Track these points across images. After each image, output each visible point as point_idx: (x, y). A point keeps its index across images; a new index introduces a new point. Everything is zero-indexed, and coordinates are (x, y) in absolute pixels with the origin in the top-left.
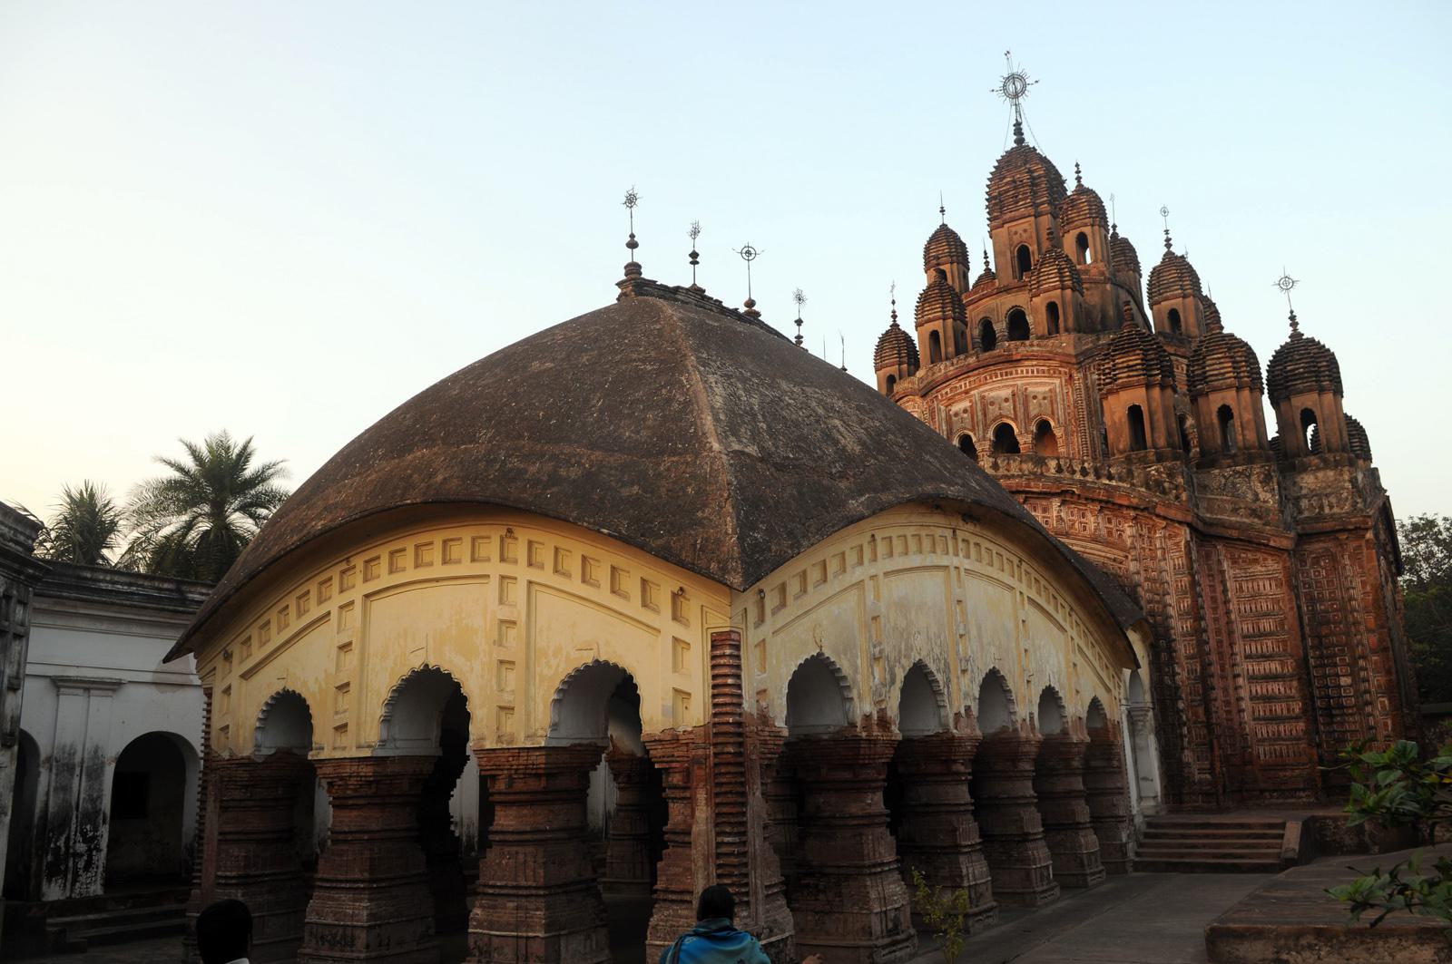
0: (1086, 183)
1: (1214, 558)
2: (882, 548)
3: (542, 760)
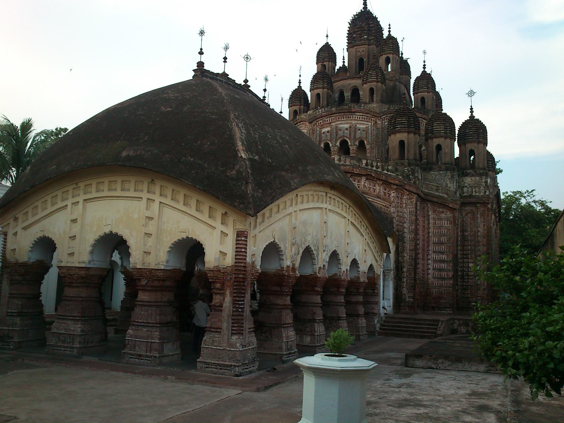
0: (393, 34)
1: (426, 209)
2: (299, 199)
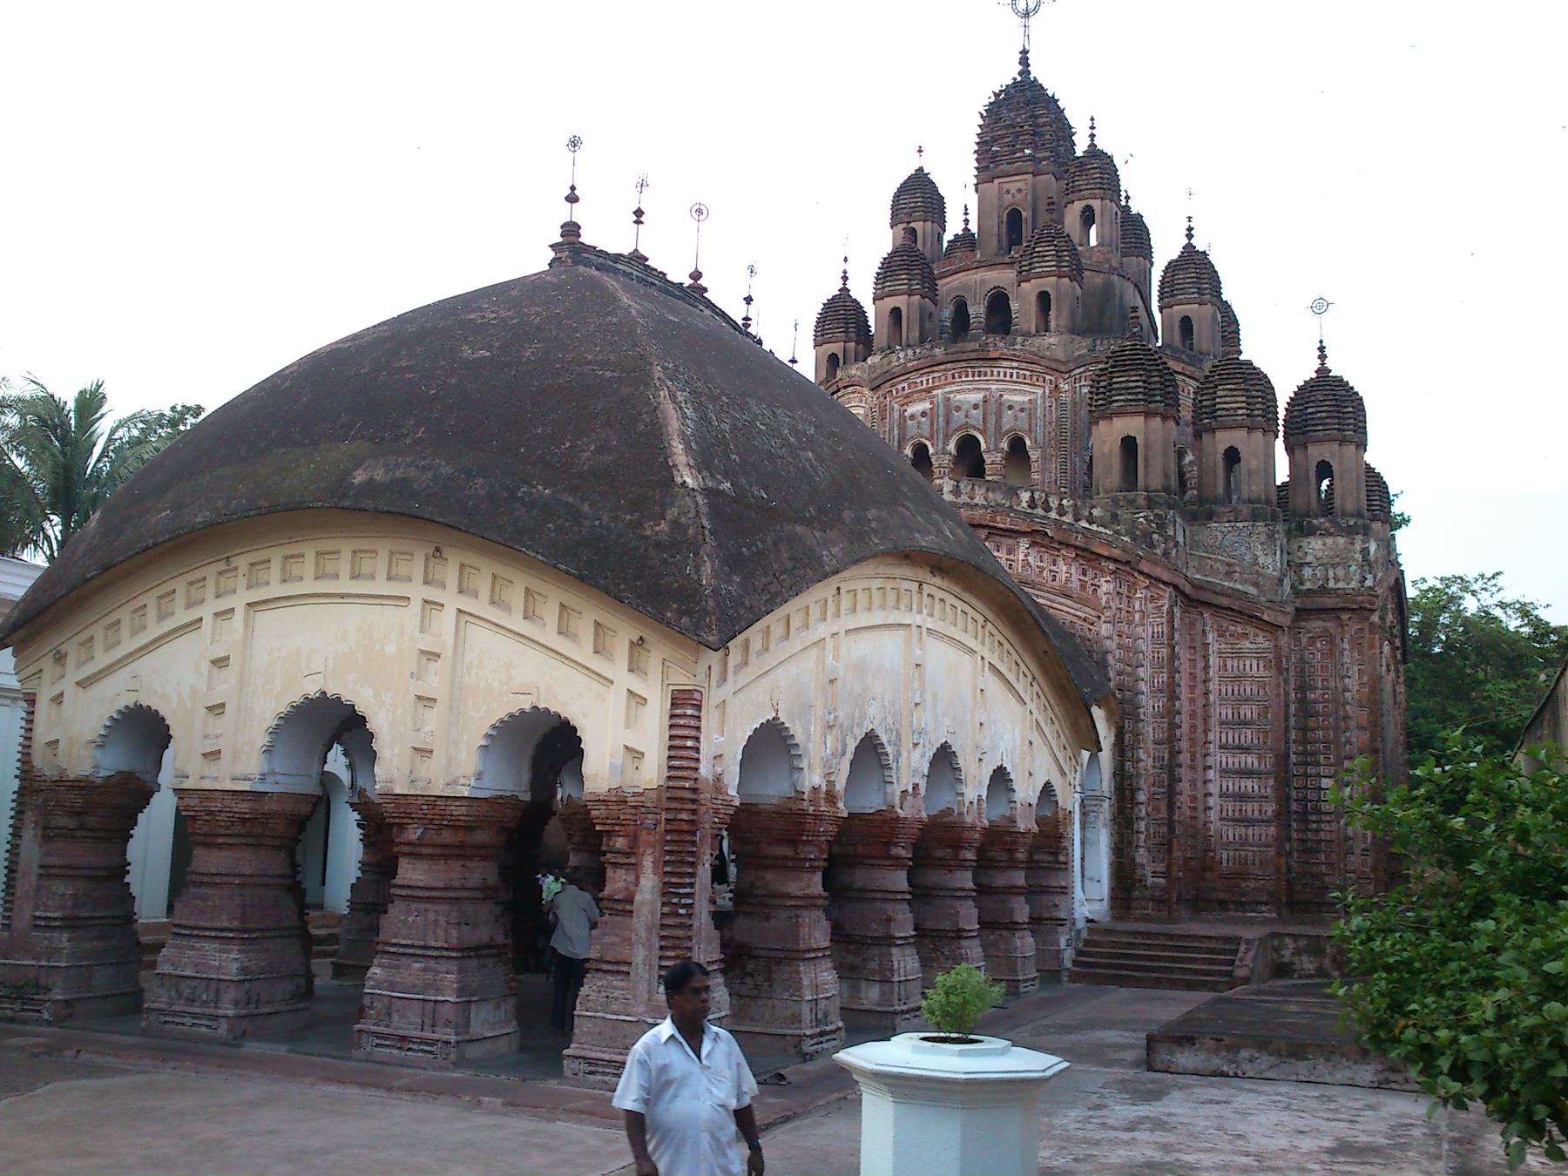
0: (1101, 144)
1: (1199, 627)
2: (846, 601)
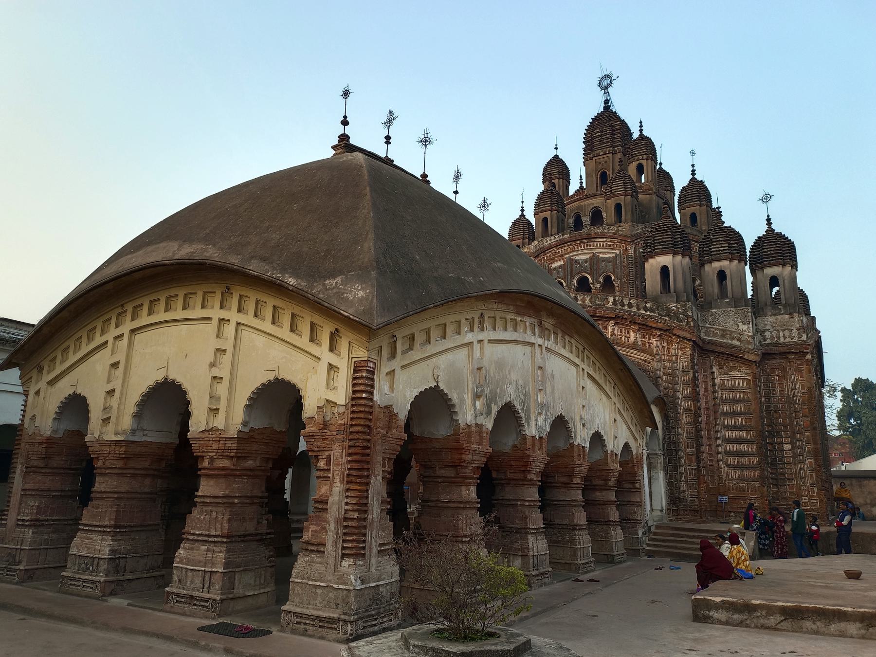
0: (645, 133)
2: (487, 323)
3: (234, 446)
